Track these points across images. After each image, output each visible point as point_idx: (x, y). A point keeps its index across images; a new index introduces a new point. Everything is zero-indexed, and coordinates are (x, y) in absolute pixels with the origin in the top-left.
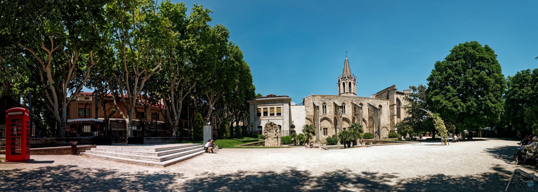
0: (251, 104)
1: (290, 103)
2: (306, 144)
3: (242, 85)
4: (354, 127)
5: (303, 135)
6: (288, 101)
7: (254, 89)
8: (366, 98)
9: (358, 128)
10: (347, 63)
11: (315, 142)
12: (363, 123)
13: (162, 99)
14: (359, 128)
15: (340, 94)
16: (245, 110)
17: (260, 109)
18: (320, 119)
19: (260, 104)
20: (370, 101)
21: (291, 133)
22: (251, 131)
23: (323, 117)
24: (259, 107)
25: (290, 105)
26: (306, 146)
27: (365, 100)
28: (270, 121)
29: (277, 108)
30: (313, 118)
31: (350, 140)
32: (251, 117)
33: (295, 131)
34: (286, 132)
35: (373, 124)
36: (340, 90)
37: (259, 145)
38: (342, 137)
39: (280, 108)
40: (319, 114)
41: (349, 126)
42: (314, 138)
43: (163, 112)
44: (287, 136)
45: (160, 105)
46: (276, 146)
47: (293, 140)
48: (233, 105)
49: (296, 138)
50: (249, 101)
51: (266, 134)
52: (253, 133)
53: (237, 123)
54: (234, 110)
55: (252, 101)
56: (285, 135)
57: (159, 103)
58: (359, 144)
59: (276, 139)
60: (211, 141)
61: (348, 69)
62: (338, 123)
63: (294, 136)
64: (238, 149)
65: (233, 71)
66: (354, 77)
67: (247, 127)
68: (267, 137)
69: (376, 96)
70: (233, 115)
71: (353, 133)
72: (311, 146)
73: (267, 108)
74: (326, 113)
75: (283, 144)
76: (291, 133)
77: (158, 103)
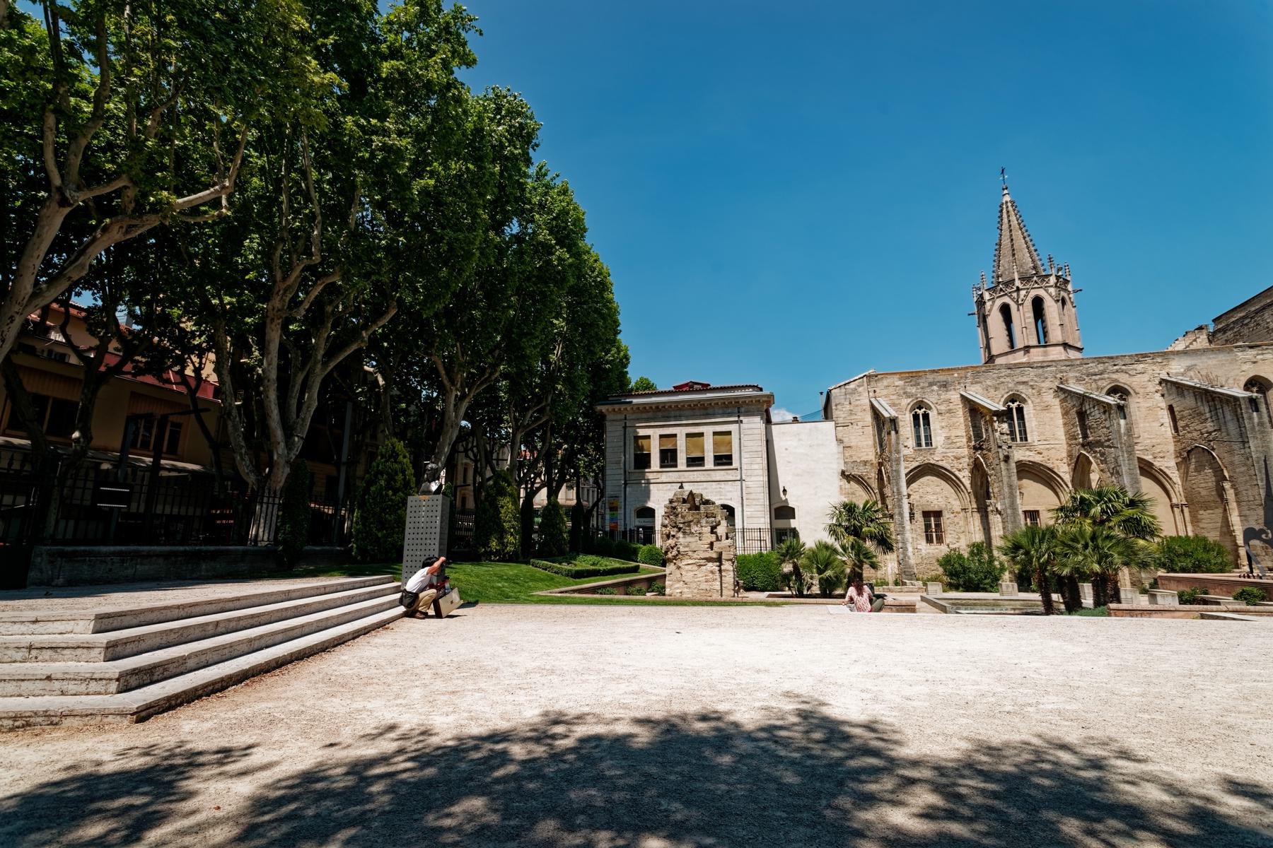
0: (610, 417)
1: (767, 412)
2: (852, 591)
3: (579, 342)
4: (1090, 505)
5: (835, 551)
6: (761, 407)
7: (624, 361)
8: (1145, 356)
9: (1117, 512)
10: (1013, 218)
11: (896, 583)
12: (1148, 487)
13: (212, 356)
14: (1129, 512)
15: (991, 359)
16: (586, 440)
17: (648, 437)
18: (903, 472)
19: (648, 420)
20: (1176, 369)
21: (780, 541)
22: (608, 529)
23: (917, 464)
24: (642, 432)
25: (768, 421)
26: (851, 599)
27: (1140, 367)
28: (687, 487)
29: (715, 433)
30: (873, 474)
31: (1077, 570)
32: (608, 472)
33: (795, 533)
34: (757, 534)
35: (1221, 491)
36: (988, 339)
37: (640, 592)
38: (1027, 553)
39: (729, 433)
40: (898, 452)
41: (1055, 503)
42: (889, 565)
43: (211, 421)
44: (761, 555)
45: (193, 384)
46: (716, 597)
47: (791, 574)
48: (538, 419)
49: (802, 561)
50: (603, 408)
51: (671, 542)
52: (618, 539)
53: (553, 493)
54: (543, 439)
55: (617, 407)
56: (753, 549)
57: (189, 372)
58: (1130, 597)
59: (712, 566)
60: (437, 564)
61: (1020, 243)
62: (994, 489)
63: (793, 552)
64: (547, 608)
65: (546, 283)
66: (1054, 272)
67: (590, 512)
68: (675, 557)
69: (1212, 337)
70: (536, 461)
71: (1094, 537)
72: (878, 603)
73: (675, 436)
74: (929, 443)
75: (747, 589)
76: (780, 541)
77: (184, 368)
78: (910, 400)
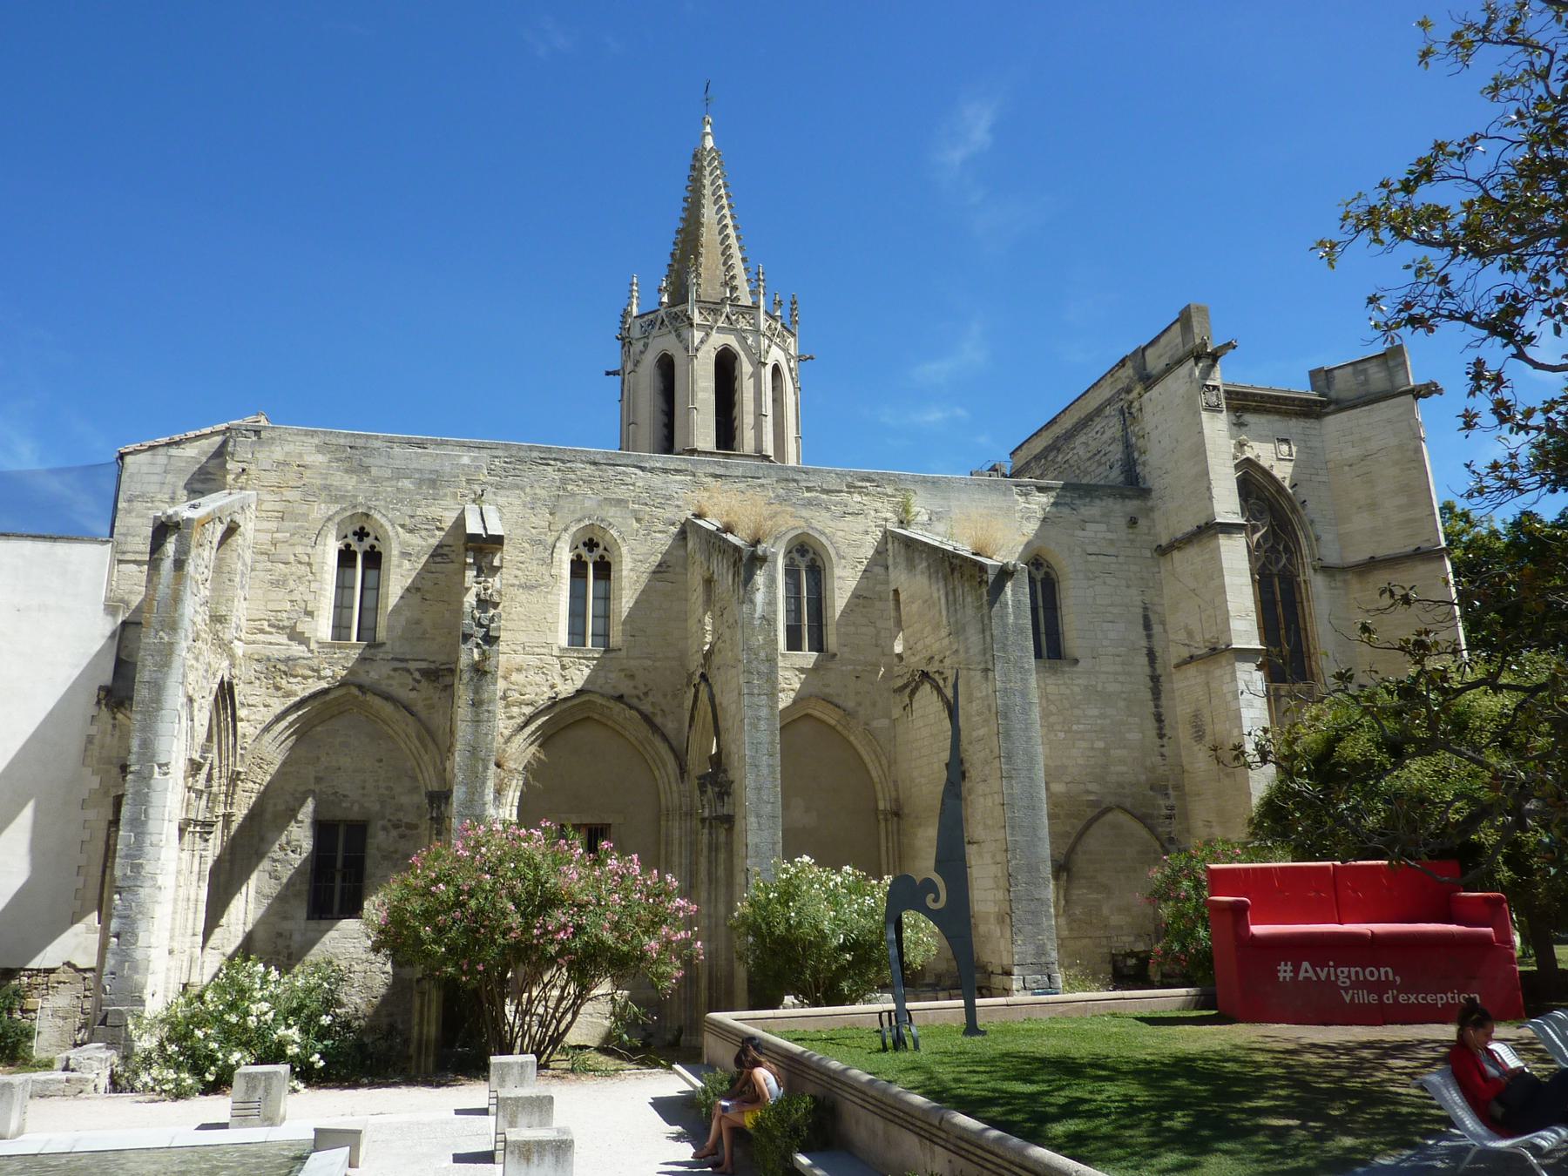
78: (335, 508)
